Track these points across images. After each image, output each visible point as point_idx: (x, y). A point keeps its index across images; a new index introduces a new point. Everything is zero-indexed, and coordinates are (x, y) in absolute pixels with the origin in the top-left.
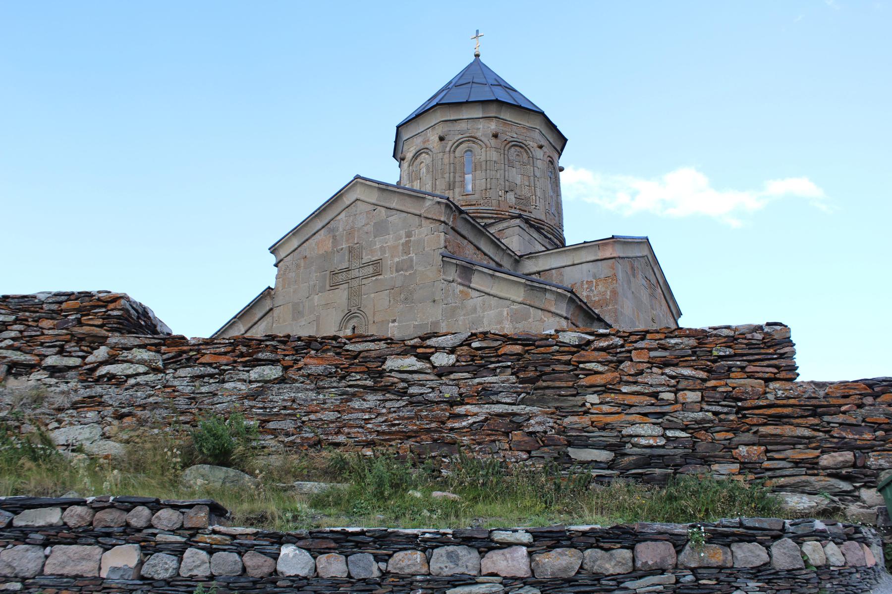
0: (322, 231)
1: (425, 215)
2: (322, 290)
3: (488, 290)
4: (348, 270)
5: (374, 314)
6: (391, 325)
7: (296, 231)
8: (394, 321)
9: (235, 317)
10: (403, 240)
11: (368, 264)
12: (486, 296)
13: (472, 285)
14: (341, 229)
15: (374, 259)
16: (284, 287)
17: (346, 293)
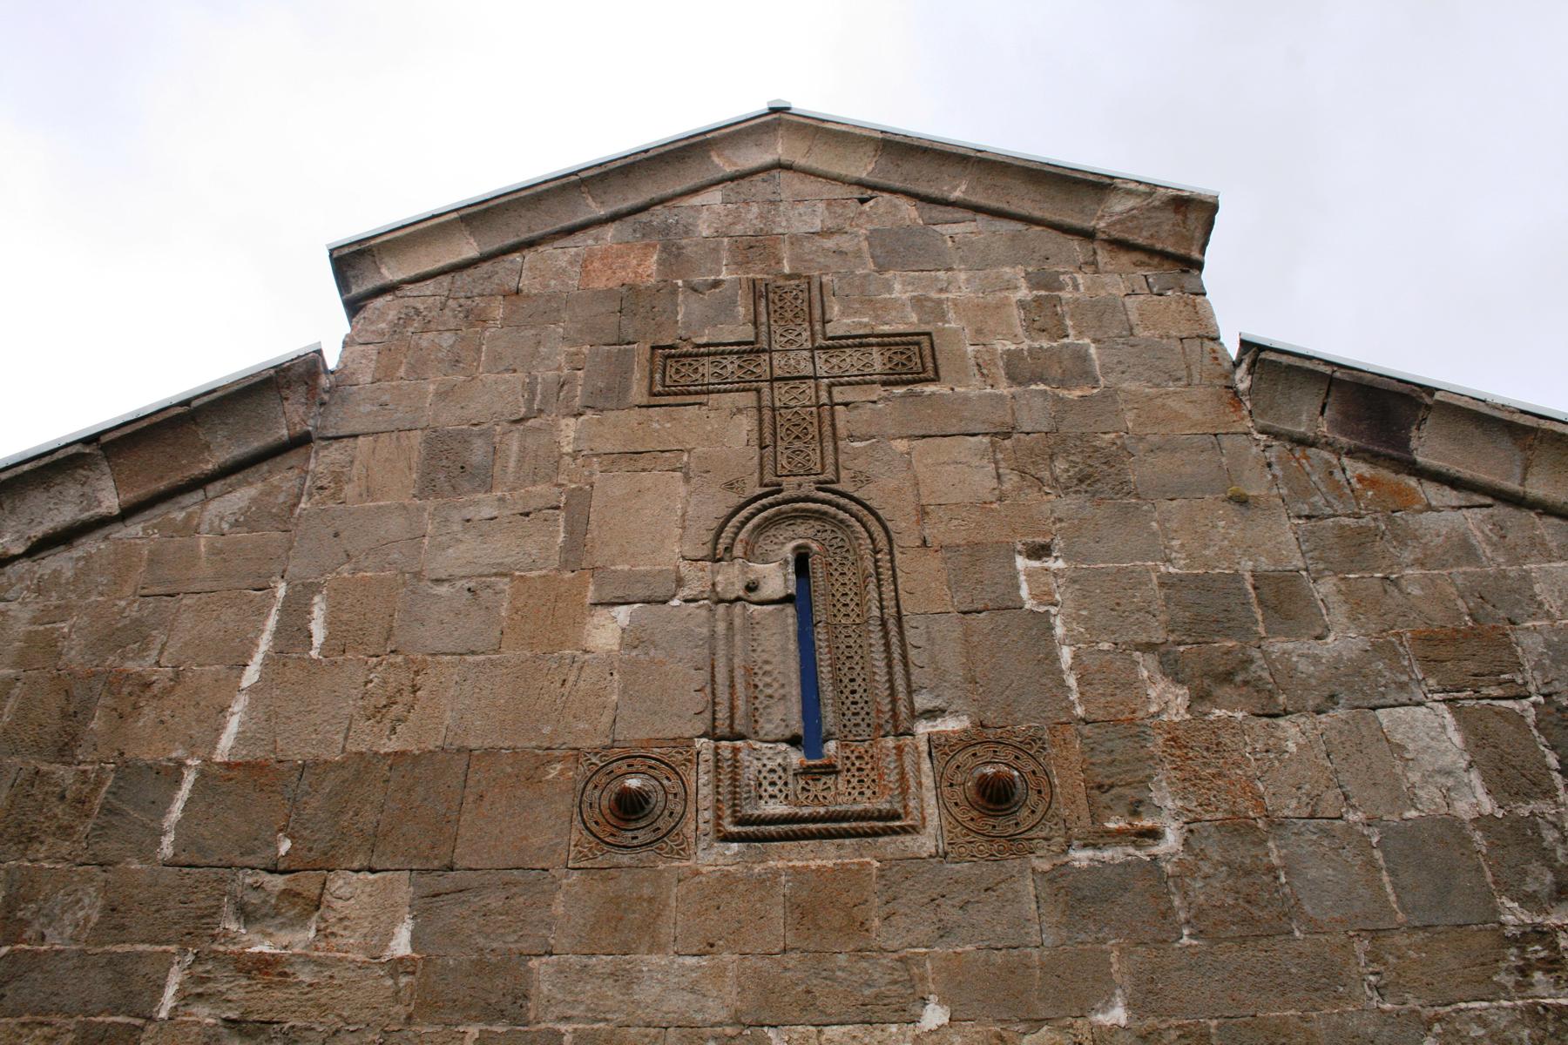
0: (610, 232)
1: (1115, 234)
2: (605, 398)
3: (1512, 485)
4: (749, 350)
5: (923, 512)
6: (1021, 562)
7: (476, 216)
8: (1039, 551)
9: (88, 440)
10: (1024, 293)
11: (860, 342)
12: (1501, 511)
13: (1419, 459)
14: (704, 230)
15: (886, 328)
16: (385, 373)
17: (745, 425)
